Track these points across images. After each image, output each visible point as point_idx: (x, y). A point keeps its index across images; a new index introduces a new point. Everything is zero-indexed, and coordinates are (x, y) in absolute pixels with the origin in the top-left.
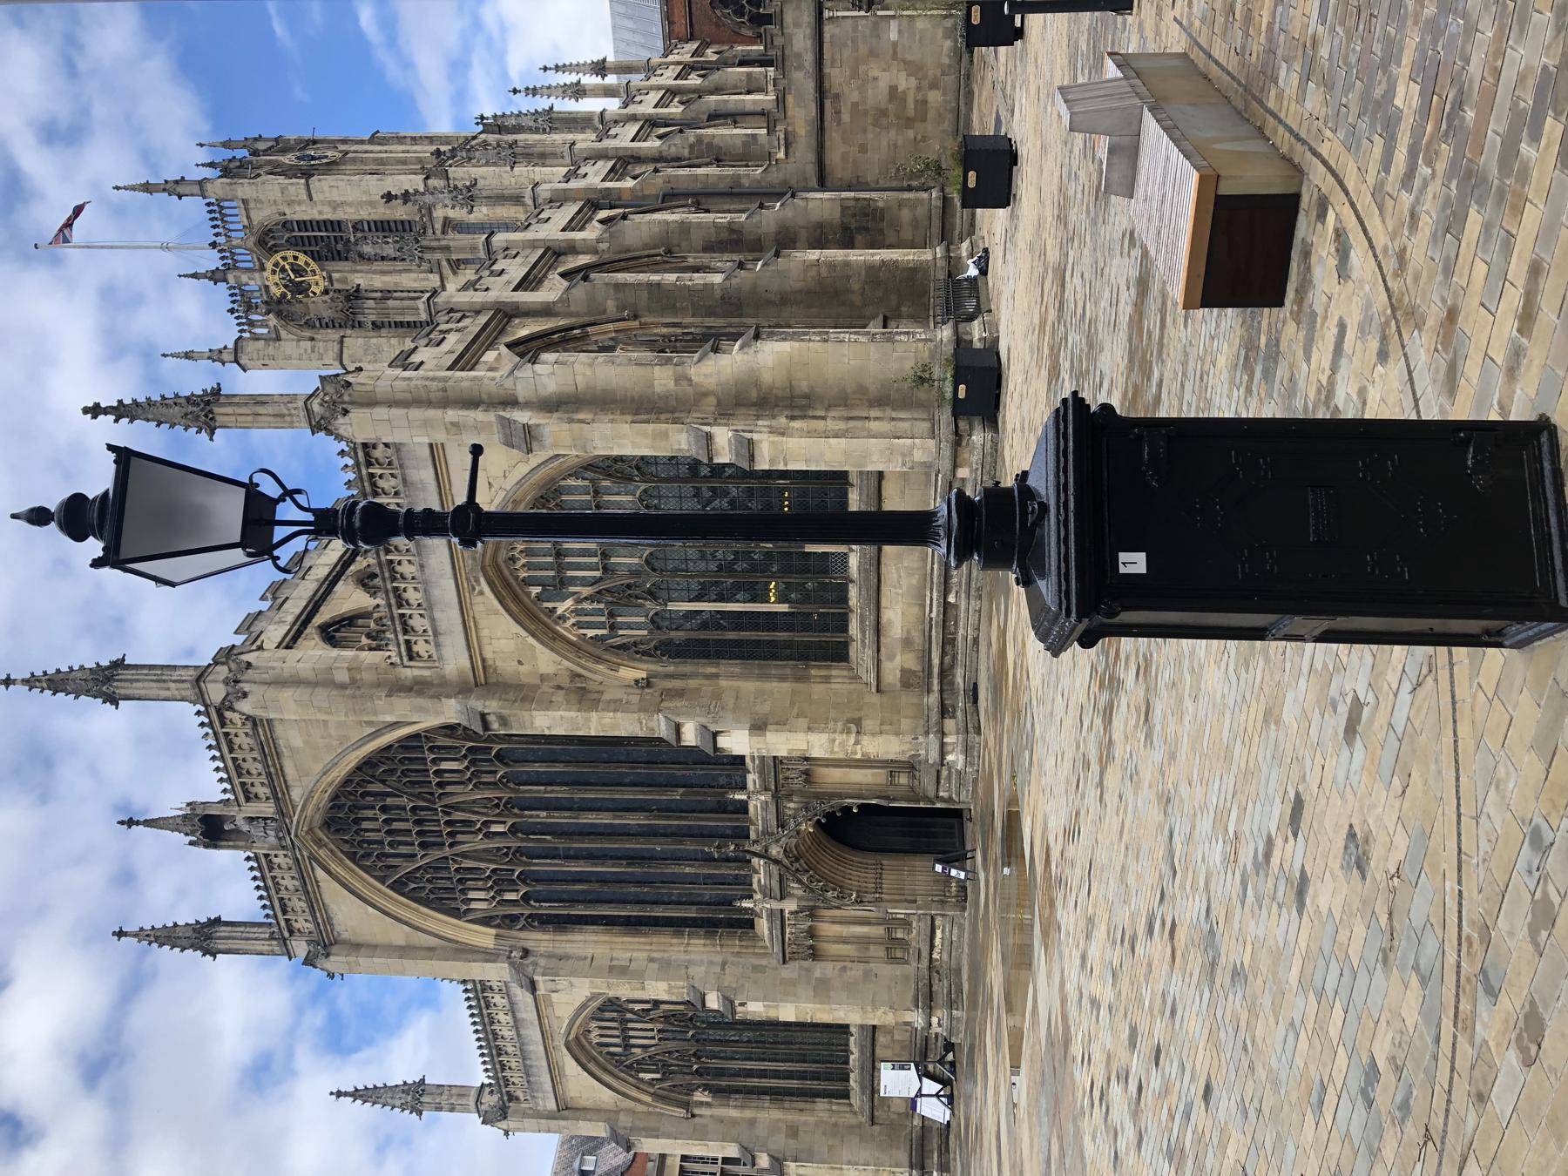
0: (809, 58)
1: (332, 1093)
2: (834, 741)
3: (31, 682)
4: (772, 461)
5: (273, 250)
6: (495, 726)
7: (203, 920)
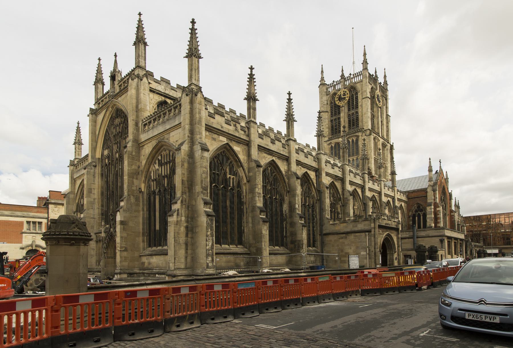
0: (356, 229)
1: (78, 121)
5: (350, 91)
7: (104, 81)
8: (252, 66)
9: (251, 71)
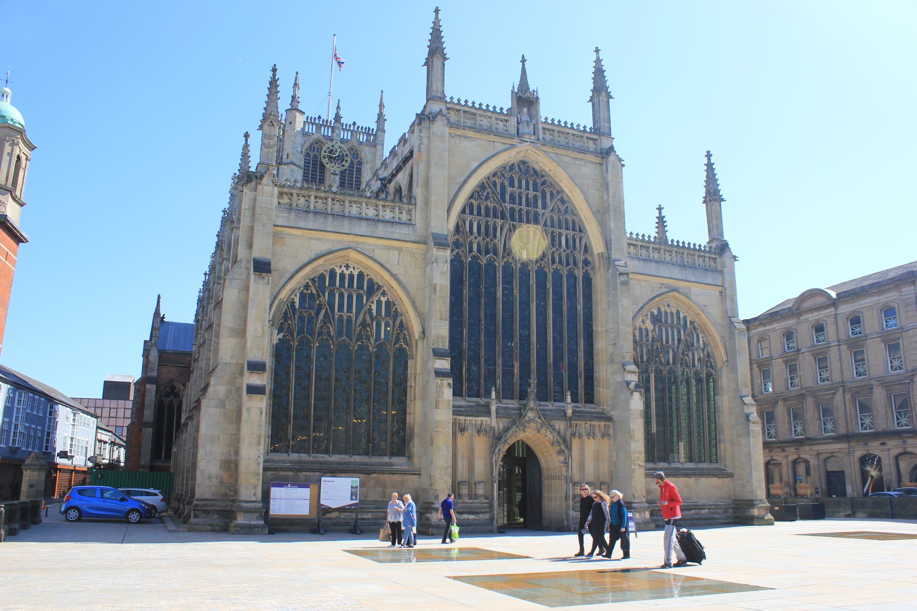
1: (275, 65)
2: (640, 454)
3: (598, 61)
4: (753, 431)
6: (622, 278)
8: (660, 206)
9: (660, 213)
